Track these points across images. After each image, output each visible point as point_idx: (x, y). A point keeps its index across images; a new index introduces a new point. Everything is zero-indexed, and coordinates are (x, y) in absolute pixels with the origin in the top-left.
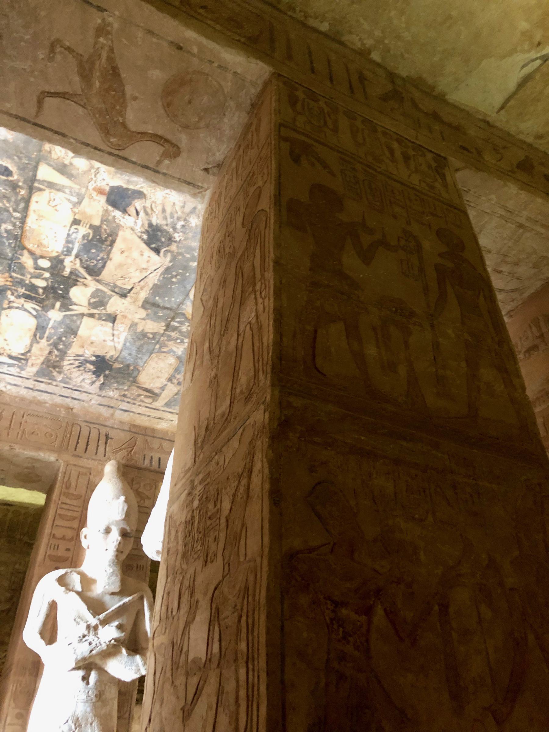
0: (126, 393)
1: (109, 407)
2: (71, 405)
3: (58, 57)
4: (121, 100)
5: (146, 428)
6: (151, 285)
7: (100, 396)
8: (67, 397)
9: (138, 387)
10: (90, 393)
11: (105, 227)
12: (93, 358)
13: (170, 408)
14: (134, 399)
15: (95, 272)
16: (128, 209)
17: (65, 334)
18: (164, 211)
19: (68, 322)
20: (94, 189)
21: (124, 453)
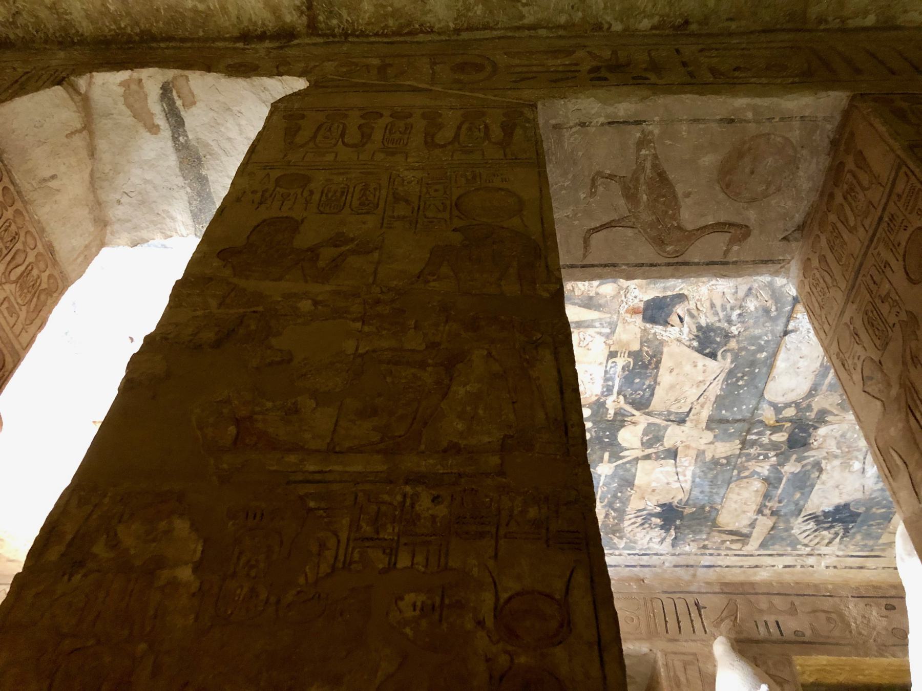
0: (706, 542)
1: (687, 566)
2: (641, 576)
3: (601, 189)
4: (673, 204)
5: (742, 584)
6: (713, 399)
7: (674, 555)
8: (634, 566)
9: (720, 532)
10: (662, 555)
11: (646, 349)
12: (659, 509)
13: (768, 549)
14: (718, 549)
15: (642, 405)
16: (668, 320)
17: (620, 488)
18: (713, 306)
19: (621, 472)
20: (627, 312)
21: (726, 625)
